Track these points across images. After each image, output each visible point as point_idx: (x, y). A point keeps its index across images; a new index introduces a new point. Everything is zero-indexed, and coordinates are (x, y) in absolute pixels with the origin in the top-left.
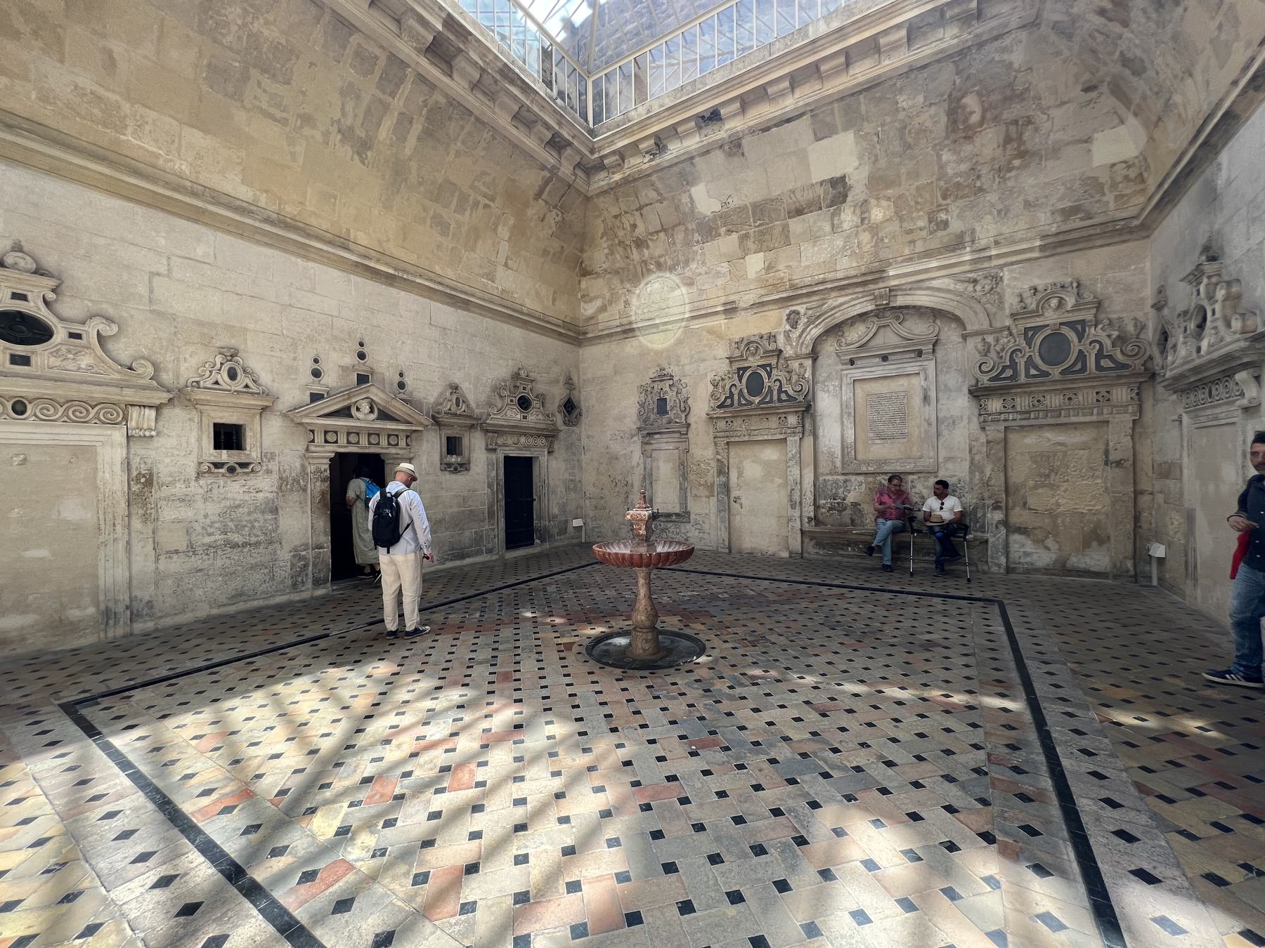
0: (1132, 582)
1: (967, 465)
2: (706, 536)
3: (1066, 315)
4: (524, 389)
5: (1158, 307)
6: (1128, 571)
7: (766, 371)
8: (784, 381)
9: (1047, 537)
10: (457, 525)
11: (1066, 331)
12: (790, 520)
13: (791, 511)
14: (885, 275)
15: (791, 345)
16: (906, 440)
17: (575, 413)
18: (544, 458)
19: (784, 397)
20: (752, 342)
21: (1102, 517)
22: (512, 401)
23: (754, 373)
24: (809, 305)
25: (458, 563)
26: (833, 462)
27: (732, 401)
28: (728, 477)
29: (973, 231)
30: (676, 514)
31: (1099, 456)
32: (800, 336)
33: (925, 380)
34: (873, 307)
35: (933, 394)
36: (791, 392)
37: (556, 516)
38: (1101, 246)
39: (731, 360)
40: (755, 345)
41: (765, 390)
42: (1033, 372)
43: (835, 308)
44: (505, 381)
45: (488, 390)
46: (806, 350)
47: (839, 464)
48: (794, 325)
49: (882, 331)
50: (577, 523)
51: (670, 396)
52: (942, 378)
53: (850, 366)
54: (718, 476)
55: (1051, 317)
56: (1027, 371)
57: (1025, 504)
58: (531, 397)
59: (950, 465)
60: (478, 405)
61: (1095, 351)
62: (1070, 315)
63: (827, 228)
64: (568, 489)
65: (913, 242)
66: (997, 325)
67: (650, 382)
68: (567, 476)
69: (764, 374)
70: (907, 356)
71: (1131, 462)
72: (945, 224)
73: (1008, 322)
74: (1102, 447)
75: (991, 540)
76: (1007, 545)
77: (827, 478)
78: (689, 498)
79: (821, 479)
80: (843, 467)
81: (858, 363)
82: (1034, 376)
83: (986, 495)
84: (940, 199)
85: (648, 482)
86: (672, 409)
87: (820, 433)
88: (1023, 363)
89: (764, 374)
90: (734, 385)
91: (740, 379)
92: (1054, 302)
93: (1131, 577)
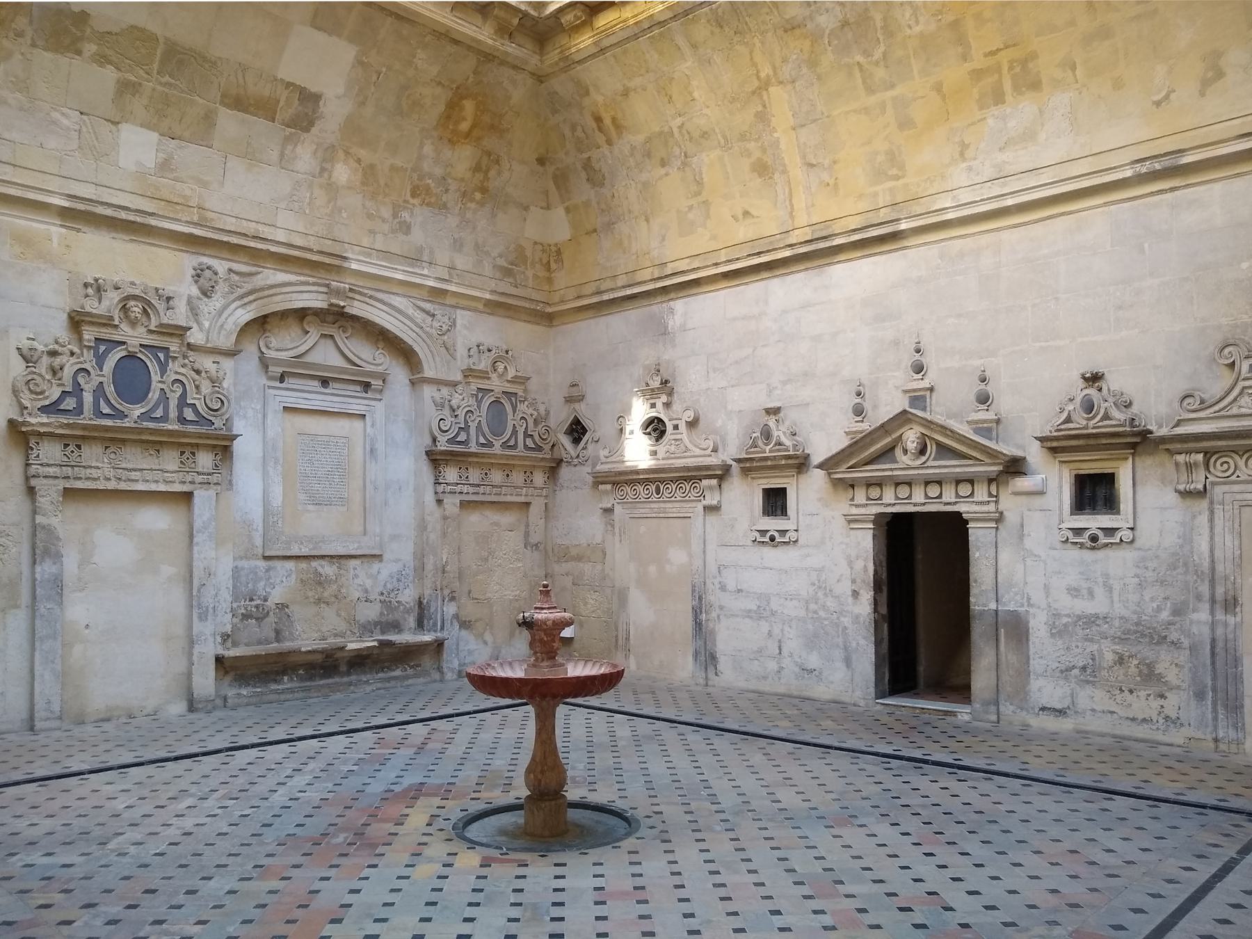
8: (190, 388)
9: (485, 630)
14: (346, 265)
16: (345, 509)
19: (189, 414)
20: (135, 297)
23: (131, 356)
24: (236, 266)
26: (250, 538)
33: (373, 425)
34: (324, 305)
35: (380, 446)
41: (154, 395)
42: (482, 440)
43: (272, 287)
47: (259, 542)
53: (278, 384)
55: (496, 384)
57: (470, 592)
65: (372, 232)
70: (352, 387)
72: (406, 228)
81: (290, 382)
82: (483, 445)
84: (409, 194)
89: (153, 367)
91: (100, 361)
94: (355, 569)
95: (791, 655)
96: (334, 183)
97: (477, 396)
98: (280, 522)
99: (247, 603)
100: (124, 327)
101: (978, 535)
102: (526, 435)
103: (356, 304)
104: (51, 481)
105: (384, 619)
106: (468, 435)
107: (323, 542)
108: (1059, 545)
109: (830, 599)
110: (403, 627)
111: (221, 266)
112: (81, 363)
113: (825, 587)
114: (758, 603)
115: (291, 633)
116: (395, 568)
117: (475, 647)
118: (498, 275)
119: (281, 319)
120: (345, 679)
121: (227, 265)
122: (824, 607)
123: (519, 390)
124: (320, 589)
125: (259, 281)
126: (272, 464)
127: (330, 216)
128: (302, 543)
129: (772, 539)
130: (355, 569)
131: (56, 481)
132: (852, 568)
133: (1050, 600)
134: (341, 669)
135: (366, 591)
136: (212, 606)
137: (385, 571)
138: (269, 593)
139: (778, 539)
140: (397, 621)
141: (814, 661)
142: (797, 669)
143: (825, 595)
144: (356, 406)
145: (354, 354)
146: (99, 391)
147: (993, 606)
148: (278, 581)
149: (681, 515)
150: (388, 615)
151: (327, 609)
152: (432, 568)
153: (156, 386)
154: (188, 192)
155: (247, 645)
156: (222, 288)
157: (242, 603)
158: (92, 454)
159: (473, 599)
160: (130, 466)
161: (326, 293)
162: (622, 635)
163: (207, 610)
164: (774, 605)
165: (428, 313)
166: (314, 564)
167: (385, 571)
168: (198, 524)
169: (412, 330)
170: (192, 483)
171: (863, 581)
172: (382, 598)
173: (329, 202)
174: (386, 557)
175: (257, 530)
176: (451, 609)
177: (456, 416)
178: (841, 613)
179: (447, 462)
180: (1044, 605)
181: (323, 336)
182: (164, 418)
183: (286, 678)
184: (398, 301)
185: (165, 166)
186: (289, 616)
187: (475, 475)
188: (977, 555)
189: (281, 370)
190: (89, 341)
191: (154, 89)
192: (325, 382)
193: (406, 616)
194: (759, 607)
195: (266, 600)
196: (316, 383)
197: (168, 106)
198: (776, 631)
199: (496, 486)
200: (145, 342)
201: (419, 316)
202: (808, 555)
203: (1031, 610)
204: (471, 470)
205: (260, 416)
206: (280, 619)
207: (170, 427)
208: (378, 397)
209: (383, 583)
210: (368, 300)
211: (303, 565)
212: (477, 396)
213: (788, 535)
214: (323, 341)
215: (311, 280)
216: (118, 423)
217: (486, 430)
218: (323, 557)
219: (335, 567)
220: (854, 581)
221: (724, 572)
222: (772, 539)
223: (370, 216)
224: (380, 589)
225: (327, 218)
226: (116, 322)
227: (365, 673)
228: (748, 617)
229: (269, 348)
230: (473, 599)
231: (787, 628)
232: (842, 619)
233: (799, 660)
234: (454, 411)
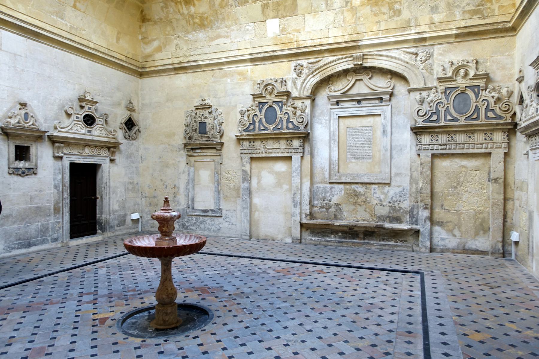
0: (501, 257)
1: (408, 179)
2: (233, 227)
3: (469, 81)
4: (89, 108)
5: (520, 80)
6: (499, 250)
7: (279, 106)
8: (291, 114)
9: (454, 228)
10: (23, 220)
12: (293, 215)
13: (293, 210)
14: (360, 44)
15: (296, 88)
16: (370, 161)
17: (136, 128)
18: (106, 165)
19: (290, 126)
21: (486, 215)
22: (78, 118)
23: (271, 106)
25: (24, 251)
26: (323, 174)
27: (255, 127)
28: (250, 183)
29: (416, 19)
30: (212, 210)
31: (485, 175)
32: (303, 83)
33: (385, 119)
34: (352, 66)
36: (295, 123)
37: (116, 211)
38: (490, 38)
39: (255, 96)
40: (271, 87)
41: (278, 120)
44: (71, 101)
45: (56, 108)
46: (307, 93)
47: (327, 176)
48: (299, 75)
49: (358, 83)
50: (135, 216)
51: (209, 121)
52: (394, 118)
53: (336, 107)
54: (243, 182)
55: (461, 82)
56: (446, 117)
57: (442, 206)
58: (96, 115)
59: (398, 179)
60: (46, 121)
61: (485, 107)
62: (471, 81)
63: (324, 6)
64: (127, 190)
65: (378, 22)
66: (429, 85)
67: (194, 109)
68: (126, 180)
69: (277, 109)
70: (373, 102)
71: (503, 180)
72: (399, 12)
73: (435, 84)
74: (487, 169)
75: (421, 230)
76: (431, 233)
77: (319, 185)
78: (222, 199)
79: (315, 186)
80: (330, 178)
81: (342, 105)
82: (450, 120)
83: (419, 199)
85: (191, 185)
86: (210, 130)
87: (316, 153)
88: (443, 112)
89: (277, 109)
90: (256, 115)
92: (462, 72)
93: (501, 254)
94: (374, 189)
96: (354, 6)
97: (445, 92)
99: (322, 202)
100: (268, 96)
103: (369, 60)
104: (246, 155)
105: (391, 215)
106: (438, 116)
107: (358, 176)
110: (402, 220)
111: (304, 63)
115: (341, 217)
116: (398, 190)
117: (446, 237)
118: (467, 16)
119: (338, 78)
120: (362, 241)
121: (307, 61)
123: (482, 83)
124: (356, 198)
127: (354, 23)
128: (347, 177)
130: (374, 189)
131: (248, 155)
134: (360, 236)
135: (381, 200)
136: (299, 202)
137: (392, 191)
138: (332, 198)
140: (399, 217)
144: (375, 111)
145: (375, 86)
146: (260, 121)
148: (336, 193)
150: (393, 213)
151: (359, 207)
152: (414, 190)
153: (279, 116)
154: (292, 37)
155: (321, 219)
156: (305, 72)
157: (320, 202)
158: (258, 144)
159: (445, 209)
160: (269, 148)
161: (352, 60)
163: (297, 204)
166: (353, 186)
167: (392, 191)
168: (294, 168)
169: (402, 65)
170: (291, 152)
172: (390, 205)
173: (353, 16)
174: (393, 183)
177: (431, 106)
179: (422, 133)
182: (281, 129)
183: (333, 236)
184: (393, 53)
185: (283, 30)
186: (340, 209)
187: (443, 138)
189: (336, 100)
191: (273, 3)
192: (359, 101)
193: (405, 215)
195: (330, 201)
196: (354, 104)
197: (279, 6)
199: (459, 144)
200: (275, 100)
201: (407, 58)
204: (440, 136)
205: (328, 122)
206: (337, 210)
207: (284, 131)
208: (388, 103)
209: (390, 197)
210: (375, 57)
211: (348, 187)
212: (445, 92)
215: (344, 56)
216: (266, 132)
219: (364, 188)
223: (375, 15)
224: (389, 200)
225: (353, 24)
226: (264, 95)
227: (373, 240)
229: (331, 92)
230: (445, 209)
234: (429, 104)
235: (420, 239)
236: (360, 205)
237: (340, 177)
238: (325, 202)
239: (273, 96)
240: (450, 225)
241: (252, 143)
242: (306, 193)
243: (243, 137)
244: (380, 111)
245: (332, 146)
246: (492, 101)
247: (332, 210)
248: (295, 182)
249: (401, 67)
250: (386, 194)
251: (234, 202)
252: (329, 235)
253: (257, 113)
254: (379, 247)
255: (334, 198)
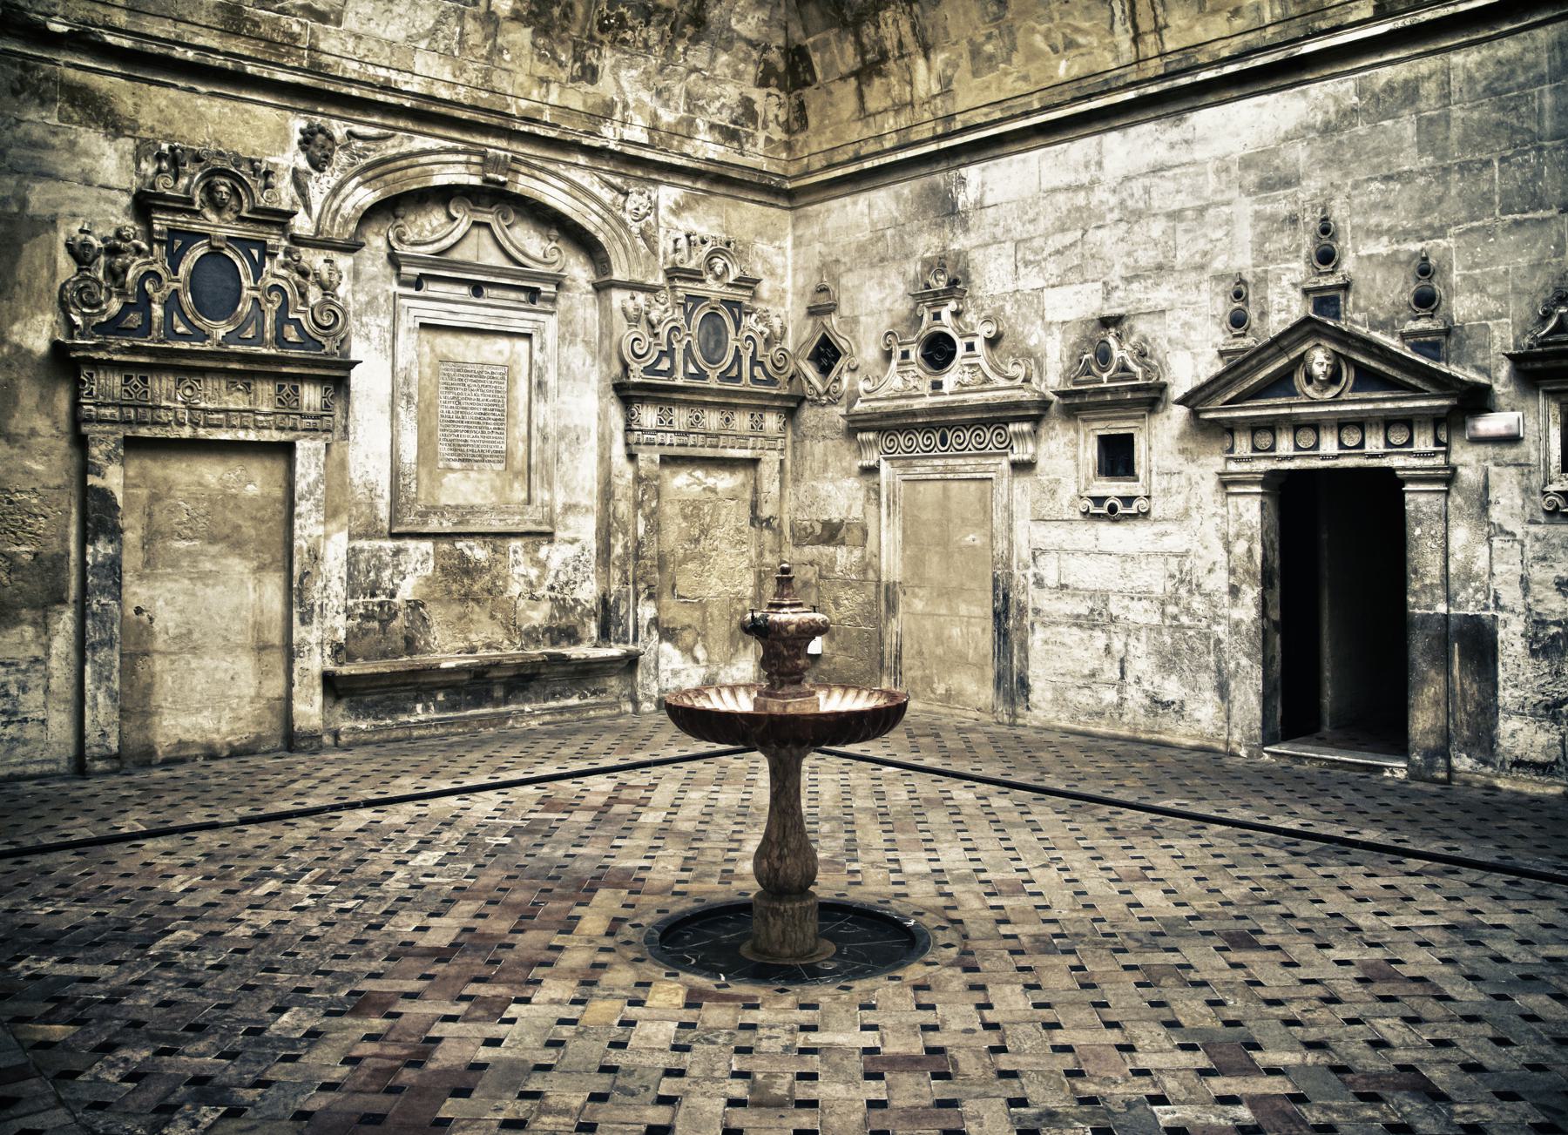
3: (724, 289)
9: (696, 642)
11: (724, 313)
15: (308, 208)
19: (292, 335)
24: (358, 129)
26: (372, 506)
27: (148, 319)
31: (746, 512)
32: (335, 192)
33: (542, 349)
34: (476, 181)
35: (551, 378)
38: (753, 201)
41: (245, 308)
42: (692, 369)
47: (384, 512)
53: (412, 291)
55: (713, 289)
57: (674, 587)
65: (544, 81)
66: (651, 281)
70: (513, 295)
74: (748, 496)
80: (393, 520)
82: (692, 376)
91: (175, 260)
94: (515, 552)
95: (1138, 681)
97: (685, 306)
98: (413, 485)
99: (368, 599)
101: (1418, 500)
102: (755, 362)
103: (521, 178)
108: (1542, 518)
109: (1197, 598)
111: (339, 129)
112: (150, 263)
113: (1190, 582)
114: (1090, 604)
115: (427, 643)
116: (571, 551)
117: (681, 666)
122: (1188, 611)
125: (390, 149)
126: (403, 403)
129: (1113, 509)
132: (1229, 552)
133: (1530, 600)
135: (530, 584)
137: (556, 555)
139: (1121, 510)
141: (1172, 689)
142: (1147, 702)
143: (1190, 591)
144: (519, 321)
147: (1441, 608)
148: (410, 568)
149: (978, 476)
151: (477, 609)
154: (296, 28)
156: (341, 158)
160: (210, 406)
162: (889, 649)
163: (312, 610)
164: (1114, 608)
165: (619, 190)
168: (301, 486)
170: (293, 429)
171: (1247, 571)
172: (553, 594)
175: (381, 497)
176: (647, 611)
178: (1215, 619)
179: (642, 400)
180: (1520, 608)
181: (476, 224)
182: (259, 340)
183: (419, 707)
184: (575, 175)
187: (681, 418)
188: (1418, 532)
189: (417, 271)
190: (161, 233)
192: (477, 288)
194: (1092, 610)
195: (393, 595)
198: (1117, 645)
200: (234, 233)
201: (607, 196)
202: (1165, 534)
203: (1501, 616)
204: (676, 411)
205: (388, 336)
206: (412, 622)
207: (265, 351)
208: (549, 307)
209: (553, 573)
210: (537, 173)
211: (445, 546)
212: (685, 306)
213: (1136, 504)
214: (475, 231)
215: (461, 146)
216: (197, 346)
217: (698, 354)
218: (471, 535)
220: (1232, 572)
221: (1041, 560)
222: (1113, 509)
226: (197, 207)
227: (528, 701)
228: (1076, 625)
230: (680, 597)
231: (1132, 641)
232: (1215, 628)
233: (1150, 688)
234: (653, 327)
235: (639, 678)
236: (477, 601)
237: (424, 515)
238: (376, 600)
239: (228, 216)
240: (688, 637)
241: (135, 381)
242: (335, 572)
243: (102, 355)
244: (530, 324)
245: (401, 411)
246: (760, 342)
247: (399, 623)
248: (306, 533)
249: (595, 218)
250: (542, 565)
251: (34, 623)
252: (409, 706)
253: (157, 267)
254: (548, 718)
255: (404, 584)
